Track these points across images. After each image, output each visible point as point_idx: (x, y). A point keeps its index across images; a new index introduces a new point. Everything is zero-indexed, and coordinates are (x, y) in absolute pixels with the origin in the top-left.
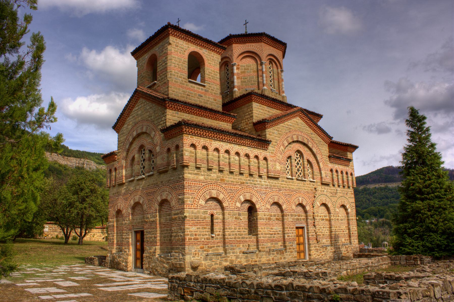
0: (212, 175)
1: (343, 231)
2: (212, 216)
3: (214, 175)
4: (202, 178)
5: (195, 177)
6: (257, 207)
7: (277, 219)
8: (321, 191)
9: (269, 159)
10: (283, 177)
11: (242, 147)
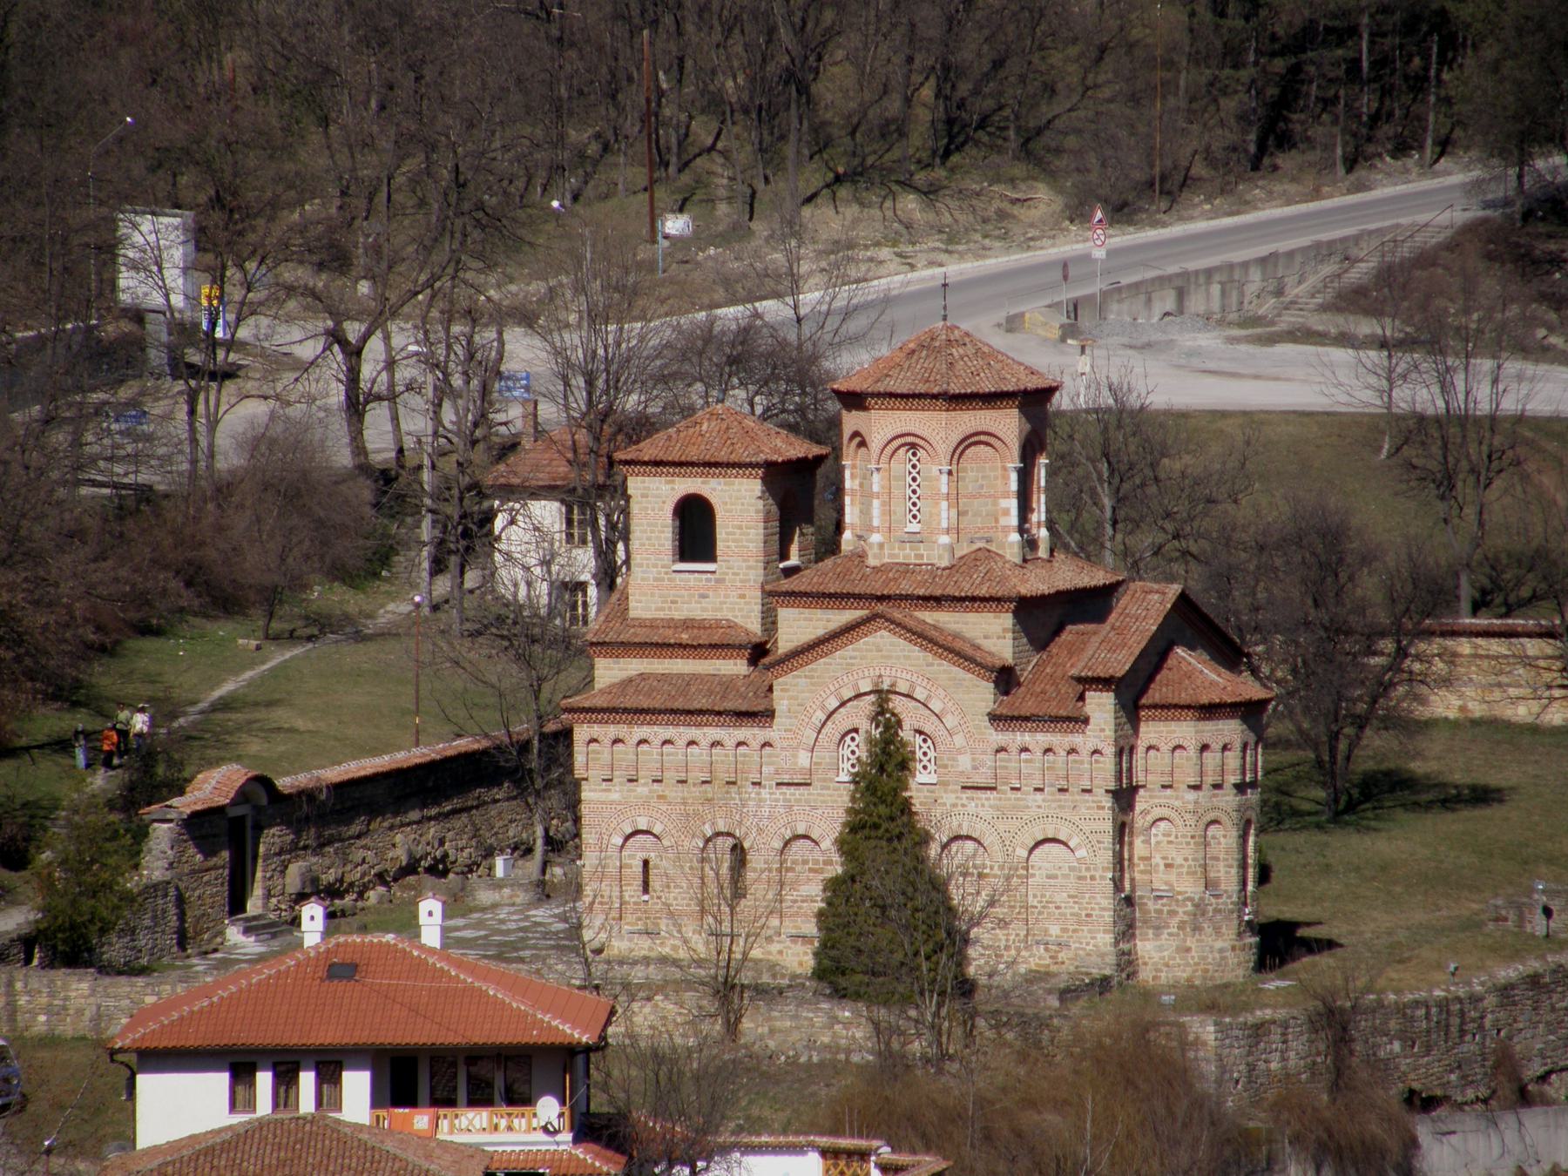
0: (639, 790)
1: (1058, 908)
2: (646, 863)
3: (642, 789)
4: (615, 796)
5: (603, 796)
6: (746, 845)
7: (811, 870)
8: (955, 805)
9: (777, 744)
10: (825, 780)
11: (706, 729)
